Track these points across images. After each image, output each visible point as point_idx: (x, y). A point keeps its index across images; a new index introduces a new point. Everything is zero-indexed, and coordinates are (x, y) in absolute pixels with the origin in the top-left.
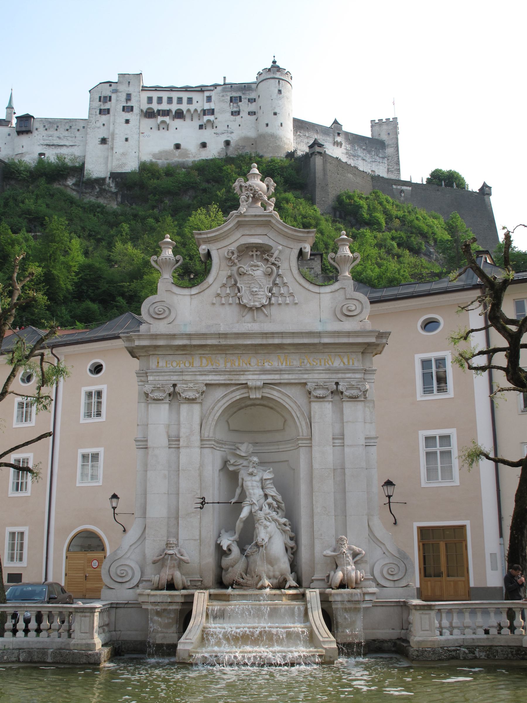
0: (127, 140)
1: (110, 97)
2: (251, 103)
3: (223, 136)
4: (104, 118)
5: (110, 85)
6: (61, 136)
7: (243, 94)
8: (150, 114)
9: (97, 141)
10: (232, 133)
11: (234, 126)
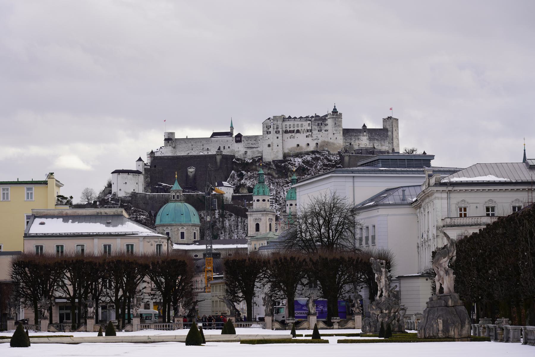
0: (278, 146)
1: (270, 126)
2: (326, 126)
3: (315, 141)
4: (269, 136)
5: (270, 121)
6: (253, 143)
7: (323, 122)
8: (286, 132)
9: (267, 146)
10: (319, 139)
11: (319, 136)
